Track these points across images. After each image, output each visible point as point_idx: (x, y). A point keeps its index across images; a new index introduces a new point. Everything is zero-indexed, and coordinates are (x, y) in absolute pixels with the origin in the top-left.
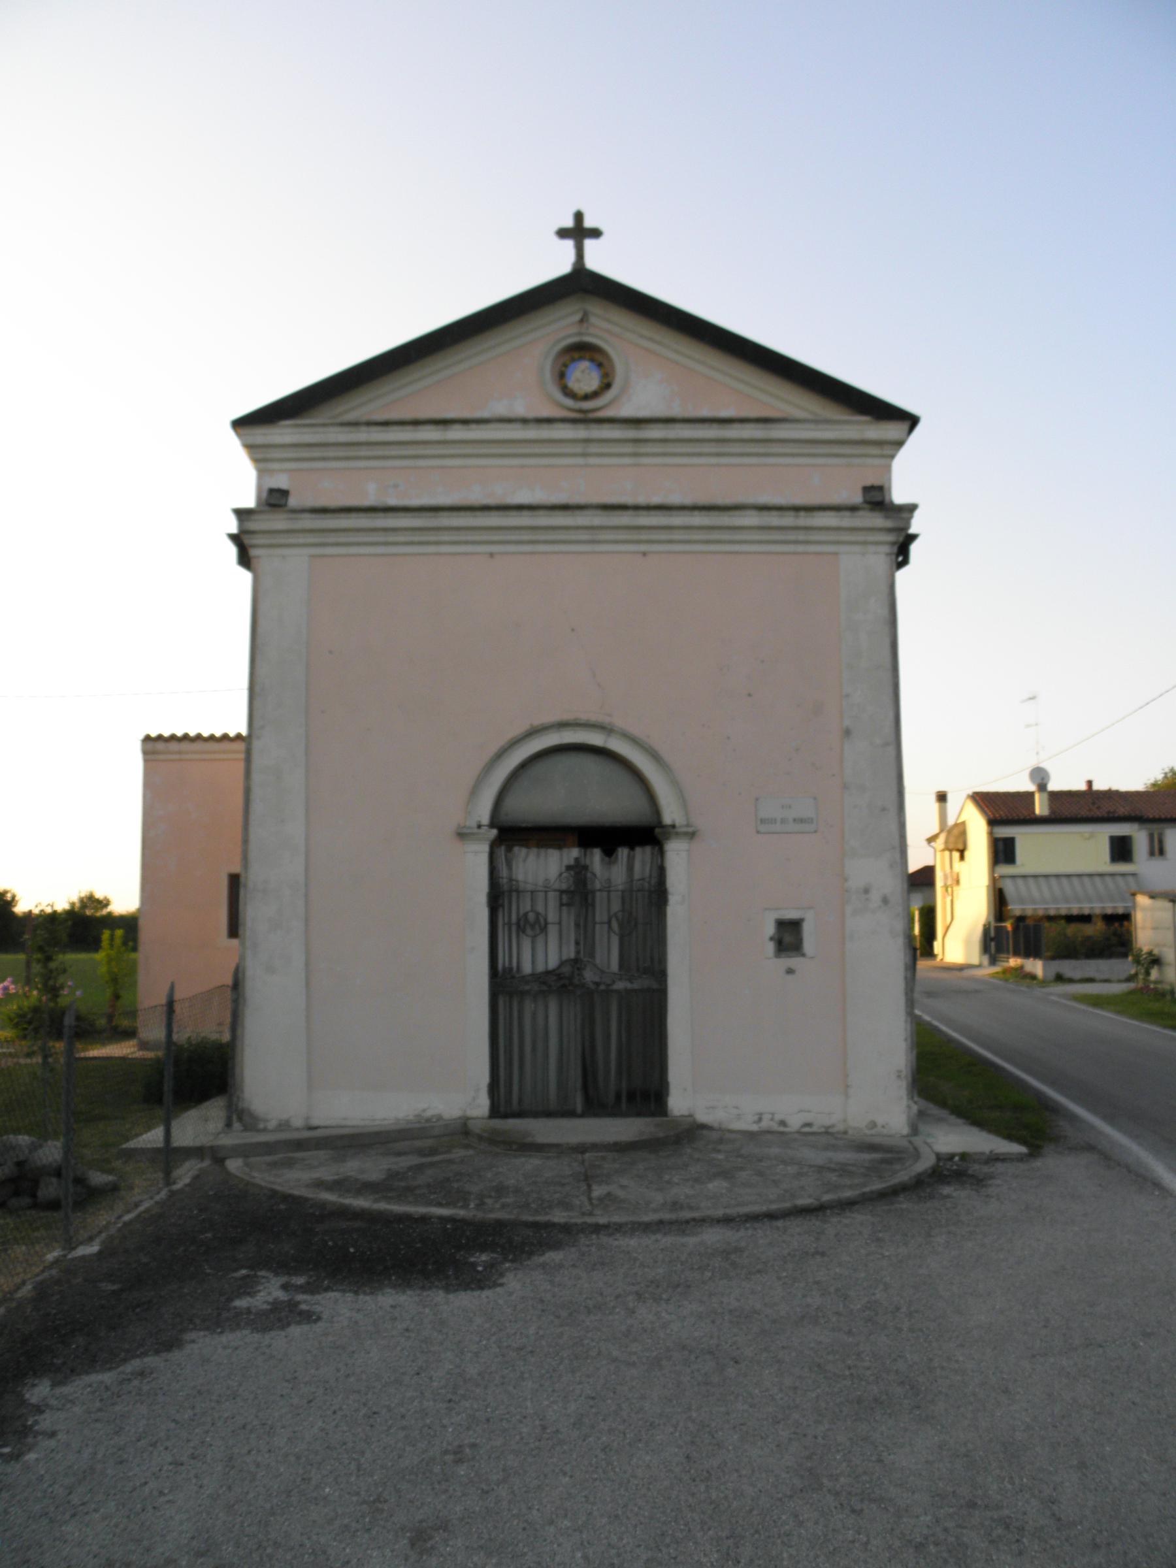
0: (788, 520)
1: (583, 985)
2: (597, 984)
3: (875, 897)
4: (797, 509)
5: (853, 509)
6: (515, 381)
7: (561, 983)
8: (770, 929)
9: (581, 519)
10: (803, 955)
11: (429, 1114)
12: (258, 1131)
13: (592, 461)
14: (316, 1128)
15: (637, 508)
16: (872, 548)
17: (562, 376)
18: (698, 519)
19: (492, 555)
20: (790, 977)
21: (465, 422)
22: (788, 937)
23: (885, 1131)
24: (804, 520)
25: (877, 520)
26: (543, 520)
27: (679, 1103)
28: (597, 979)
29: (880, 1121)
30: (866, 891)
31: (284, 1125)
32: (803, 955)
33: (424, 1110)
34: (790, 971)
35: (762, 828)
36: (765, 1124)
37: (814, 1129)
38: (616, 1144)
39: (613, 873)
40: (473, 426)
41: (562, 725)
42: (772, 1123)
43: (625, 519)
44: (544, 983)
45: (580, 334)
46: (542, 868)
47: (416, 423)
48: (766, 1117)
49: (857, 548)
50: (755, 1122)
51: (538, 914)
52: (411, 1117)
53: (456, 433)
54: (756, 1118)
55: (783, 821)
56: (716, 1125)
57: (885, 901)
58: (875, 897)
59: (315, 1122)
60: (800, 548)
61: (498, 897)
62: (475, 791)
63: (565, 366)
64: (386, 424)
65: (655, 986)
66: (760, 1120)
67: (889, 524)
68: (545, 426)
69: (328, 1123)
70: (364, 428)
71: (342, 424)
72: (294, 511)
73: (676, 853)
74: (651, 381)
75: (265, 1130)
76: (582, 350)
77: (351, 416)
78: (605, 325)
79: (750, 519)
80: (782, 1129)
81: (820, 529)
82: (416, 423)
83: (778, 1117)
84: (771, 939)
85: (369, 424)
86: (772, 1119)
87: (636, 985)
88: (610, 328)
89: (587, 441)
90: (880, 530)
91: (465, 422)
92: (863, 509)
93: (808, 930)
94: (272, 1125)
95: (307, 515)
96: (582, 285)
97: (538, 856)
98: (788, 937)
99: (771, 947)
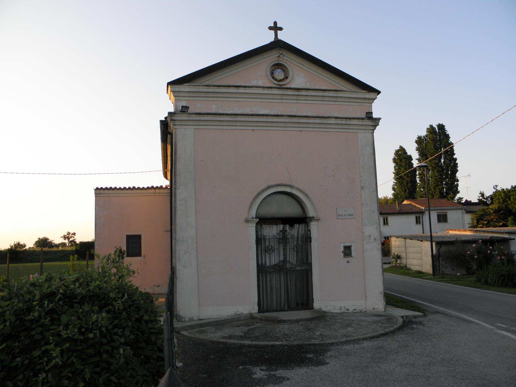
0: (344, 122)
2: (291, 268)
3: (372, 238)
4: (346, 118)
5: (363, 119)
6: (258, 74)
7: (280, 268)
8: (342, 249)
11: (238, 313)
13: (284, 101)
14: (201, 320)
15: (299, 116)
16: (367, 131)
18: (317, 121)
19: (253, 130)
22: (347, 251)
24: (348, 122)
26: (270, 119)
29: (376, 308)
30: (370, 236)
31: (191, 320)
34: (348, 262)
35: (339, 217)
36: (342, 310)
37: (357, 311)
38: (308, 318)
40: (247, 88)
43: (295, 120)
46: (272, 231)
47: (229, 86)
48: (343, 308)
49: (363, 131)
51: (272, 246)
53: (241, 90)
56: (328, 311)
57: (375, 239)
58: (372, 238)
59: (201, 318)
60: (347, 131)
61: (259, 241)
63: (273, 70)
67: (373, 124)
68: (270, 89)
70: (212, 87)
71: (205, 86)
72: (189, 114)
73: (313, 226)
74: (300, 77)
75: (185, 321)
76: (278, 66)
77: (206, 83)
82: (229, 86)
83: (346, 308)
85: (214, 86)
87: (303, 268)
88: (288, 60)
93: (353, 249)
94: (186, 320)
95: (194, 115)
96: (278, 45)
98: (347, 251)
99: (342, 254)
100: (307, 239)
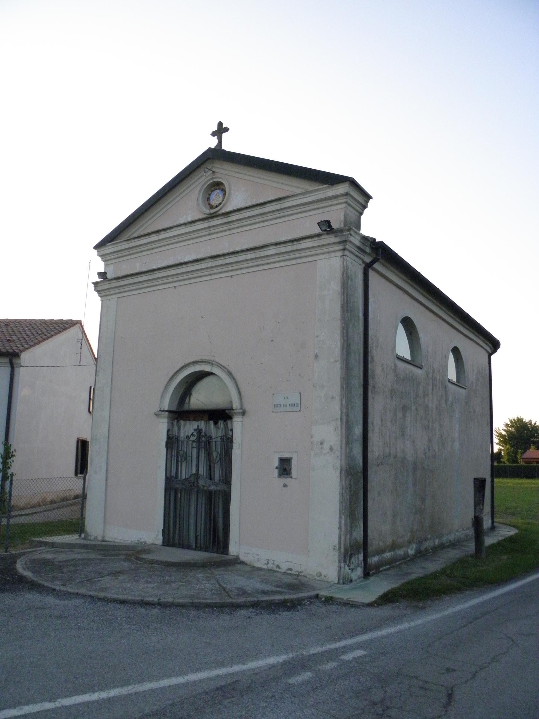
0: (289, 248)
1: (198, 486)
2: (204, 486)
3: (326, 446)
4: (292, 241)
5: (318, 235)
6: (188, 206)
7: (192, 484)
8: (276, 463)
9: (204, 265)
10: (291, 477)
11: (141, 541)
12: (88, 540)
13: (213, 236)
14: (105, 541)
15: (224, 255)
16: (333, 254)
17: (208, 199)
18: (250, 255)
19: (175, 287)
20: (285, 488)
21: (165, 230)
22: (285, 467)
23: (326, 579)
24: (296, 246)
25: (332, 239)
26: (191, 268)
27: (233, 549)
28: (204, 484)
29: (324, 573)
30: (322, 443)
31: (96, 538)
32: (291, 477)
33: (140, 539)
34: (285, 486)
35: (277, 409)
36: (270, 566)
37: (293, 572)
38: (166, 562)
39: (214, 431)
40: (168, 231)
41: (195, 363)
42: (273, 566)
43: (220, 261)
44: (183, 484)
45: (213, 178)
47: (149, 234)
48: (271, 562)
49: (326, 256)
50: (265, 564)
51: (184, 451)
52: (136, 541)
53: (163, 235)
54: (266, 562)
55: (285, 406)
56: (248, 563)
57: (331, 449)
58: (326, 446)
59: (107, 539)
60: (299, 261)
61: (172, 442)
62: (163, 396)
63: (210, 195)
64: (139, 237)
65: (226, 489)
66: (268, 563)
67: (337, 240)
68: (193, 225)
69: (110, 540)
70: (133, 241)
71: (126, 241)
72: (110, 280)
73: (237, 422)
74: (241, 191)
75: (90, 540)
76: (218, 185)
77: (136, 235)
78: (223, 171)
79: (272, 251)
80: (277, 569)
81: (305, 249)
82: (149, 234)
83: (276, 563)
84: (277, 468)
85: (134, 238)
86: (273, 564)
87: (218, 488)
88: (224, 172)
89: (209, 228)
90: (334, 243)
91: (165, 230)
92: (324, 234)
93: (294, 463)
94: (92, 538)
95: (114, 281)
96: (215, 156)
97: (190, 424)
98: (285, 467)
99: (276, 472)
100: (228, 442)
